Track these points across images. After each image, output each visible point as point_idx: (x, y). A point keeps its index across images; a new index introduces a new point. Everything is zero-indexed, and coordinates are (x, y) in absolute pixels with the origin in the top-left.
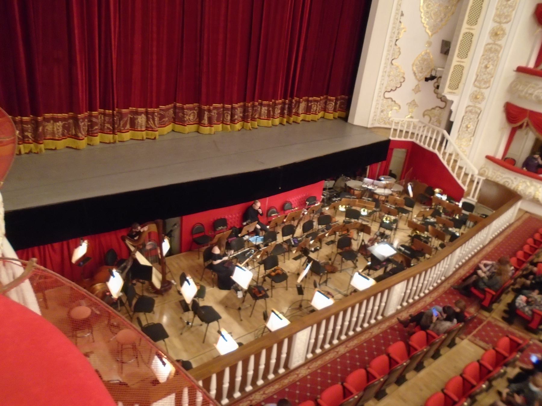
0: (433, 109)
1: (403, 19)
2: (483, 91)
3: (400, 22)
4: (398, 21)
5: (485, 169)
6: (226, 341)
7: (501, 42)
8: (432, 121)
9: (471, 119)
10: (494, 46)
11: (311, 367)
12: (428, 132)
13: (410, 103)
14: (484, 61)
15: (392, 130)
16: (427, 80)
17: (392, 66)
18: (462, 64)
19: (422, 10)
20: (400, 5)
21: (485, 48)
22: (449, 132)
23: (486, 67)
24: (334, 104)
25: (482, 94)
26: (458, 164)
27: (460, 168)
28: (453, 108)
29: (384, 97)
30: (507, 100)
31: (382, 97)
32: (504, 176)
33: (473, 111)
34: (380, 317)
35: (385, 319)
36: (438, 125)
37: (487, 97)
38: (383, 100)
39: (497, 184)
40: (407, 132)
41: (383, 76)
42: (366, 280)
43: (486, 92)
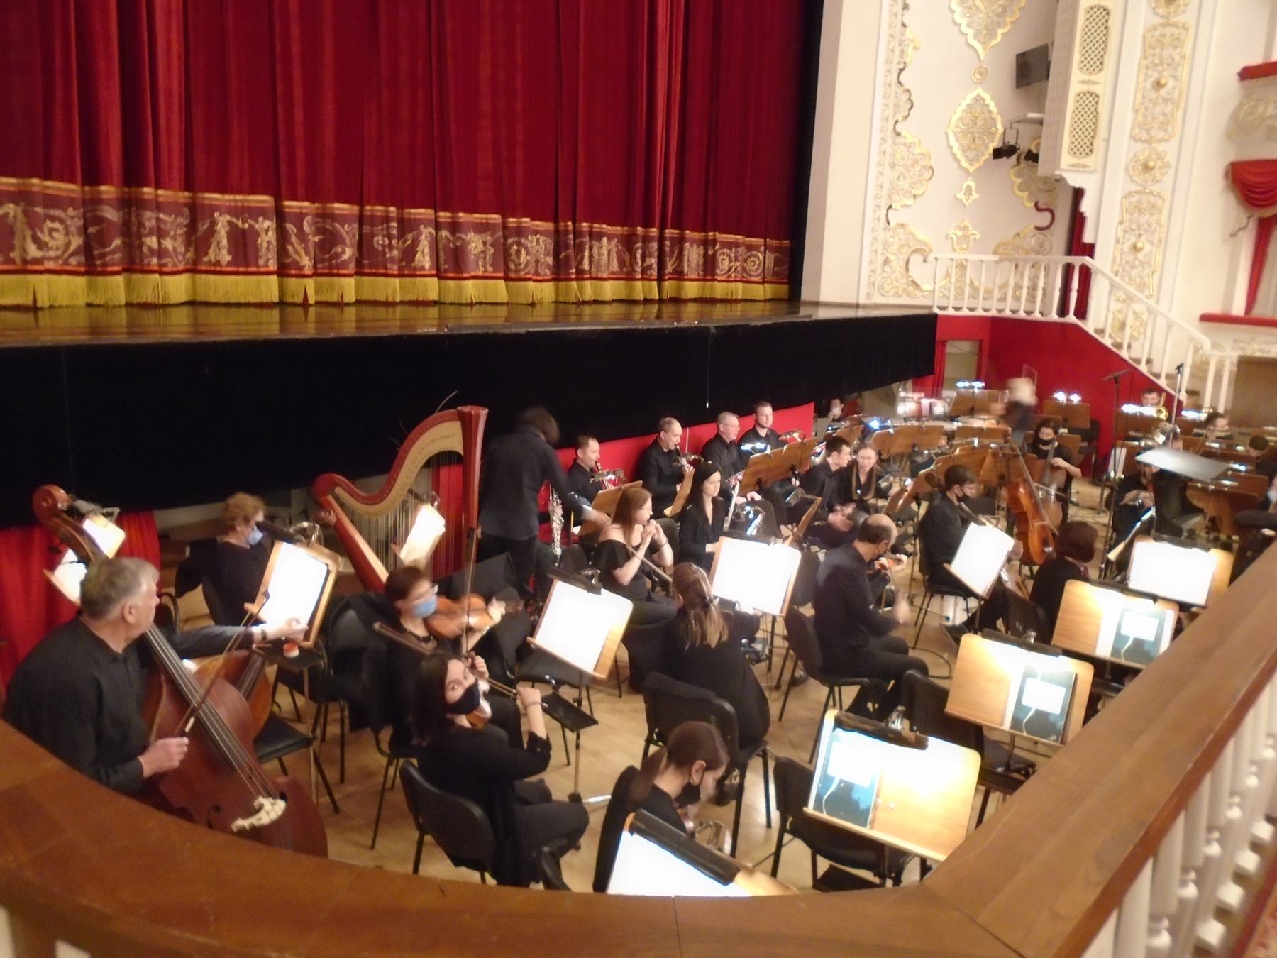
1: (908, 17)
2: (1161, 148)
3: (904, 25)
4: (899, 24)
9: (1139, 227)
10: (1168, 31)
14: (1150, 72)
16: (998, 153)
17: (899, 140)
18: (1093, 88)
21: (1144, 37)
23: (1158, 85)
25: (1160, 157)
28: (1086, 207)
30: (1232, 157)
41: (880, 164)
43: (1169, 150)
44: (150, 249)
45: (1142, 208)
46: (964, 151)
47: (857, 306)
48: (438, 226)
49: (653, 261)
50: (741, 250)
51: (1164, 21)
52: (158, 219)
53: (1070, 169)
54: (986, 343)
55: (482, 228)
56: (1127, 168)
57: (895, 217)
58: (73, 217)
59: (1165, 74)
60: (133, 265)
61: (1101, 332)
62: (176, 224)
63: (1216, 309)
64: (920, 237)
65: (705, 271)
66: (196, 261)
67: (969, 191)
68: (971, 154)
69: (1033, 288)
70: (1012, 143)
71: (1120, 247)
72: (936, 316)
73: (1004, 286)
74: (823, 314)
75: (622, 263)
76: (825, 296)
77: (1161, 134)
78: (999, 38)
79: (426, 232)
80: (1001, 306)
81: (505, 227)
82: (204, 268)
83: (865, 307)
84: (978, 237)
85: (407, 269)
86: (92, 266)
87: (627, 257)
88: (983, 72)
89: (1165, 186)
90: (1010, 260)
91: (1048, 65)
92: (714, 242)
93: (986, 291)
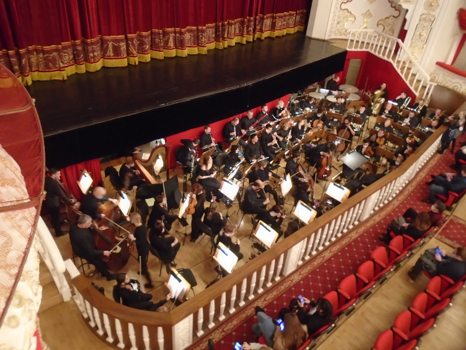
0: (387, 18)
5: (435, 75)
6: (227, 255)
8: (385, 31)
9: (424, 27)
11: (302, 273)
12: (383, 41)
13: (365, 13)
15: (349, 41)
22: (403, 41)
26: (412, 72)
27: (414, 75)
28: (408, 17)
29: (341, 9)
31: (339, 9)
32: (454, 81)
33: (427, 19)
34: (356, 223)
35: (361, 224)
36: (392, 34)
37: (441, 5)
38: (339, 11)
39: (448, 89)
40: (363, 43)
42: (341, 189)
44: (91, 57)
48: (175, 33)
49: (251, 29)
50: (287, 18)
52: (93, 48)
55: (190, 31)
58: (70, 51)
60: (87, 60)
62: (97, 47)
65: (272, 27)
72: (346, 52)
75: (240, 30)
79: (172, 35)
81: (197, 29)
85: (166, 47)
86: (76, 61)
87: (242, 28)
92: (275, 18)
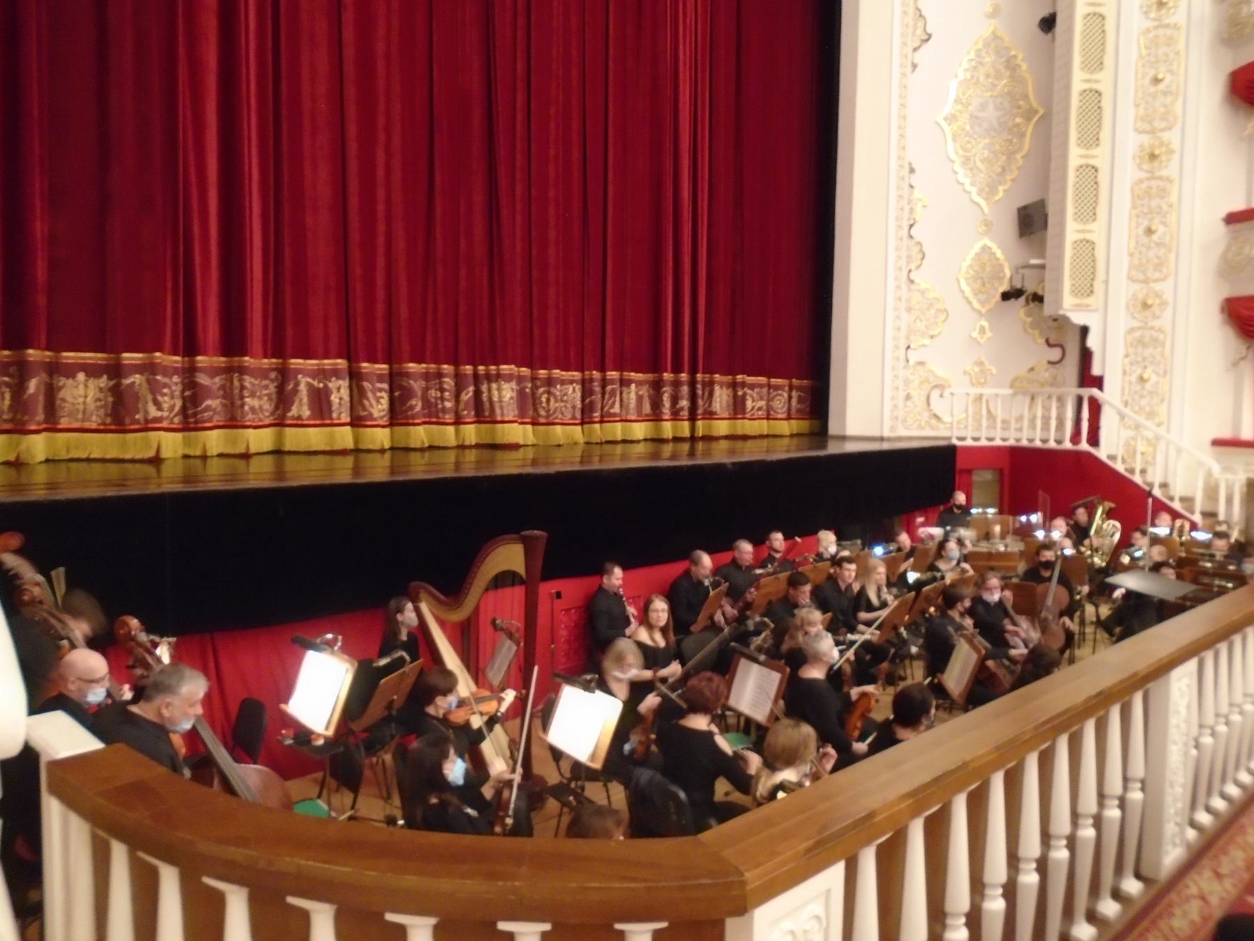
1: (914, 179)
2: (1157, 287)
3: (911, 187)
4: (907, 186)
7: (1171, 170)
9: (1144, 359)
10: (1154, 183)
16: (1006, 296)
17: (913, 287)
18: (1088, 236)
19: (954, 157)
20: (904, 148)
21: (1132, 191)
23: (1149, 231)
24: (786, 395)
25: (1158, 295)
28: (1092, 342)
30: (1227, 292)
41: (895, 309)
43: (1166, 288)
45: (1146, 342)
46: (975, 295)
47: (882, 439)
49: (684, 403)
51: (1148, 175)
53: (1073, 309)
54: (1006, 472)
56: (1127, 306)
57: (912, 356)
59: (1156, 221)
61: (1110, 457)
63: (1226, 434)
64: (940, 373)
66: (283, 417)
67: (982, 330)
68: (982, 297)
69: (1046, 420)
70: (1019, 286)
71: (1127, 378)
73: (1020, 419)
74: (851, 447)
76: (852, 429)
77: (1157, 275)
78: (1001, 194)
80: (1018, 435)
82: (289, 422)
83: (889, 439)
84: (994, 371)
88: (987, 224)
89: (1165, 320)
90: (1024, 393)
91: (1046, 216)
93: (1004, 422)
